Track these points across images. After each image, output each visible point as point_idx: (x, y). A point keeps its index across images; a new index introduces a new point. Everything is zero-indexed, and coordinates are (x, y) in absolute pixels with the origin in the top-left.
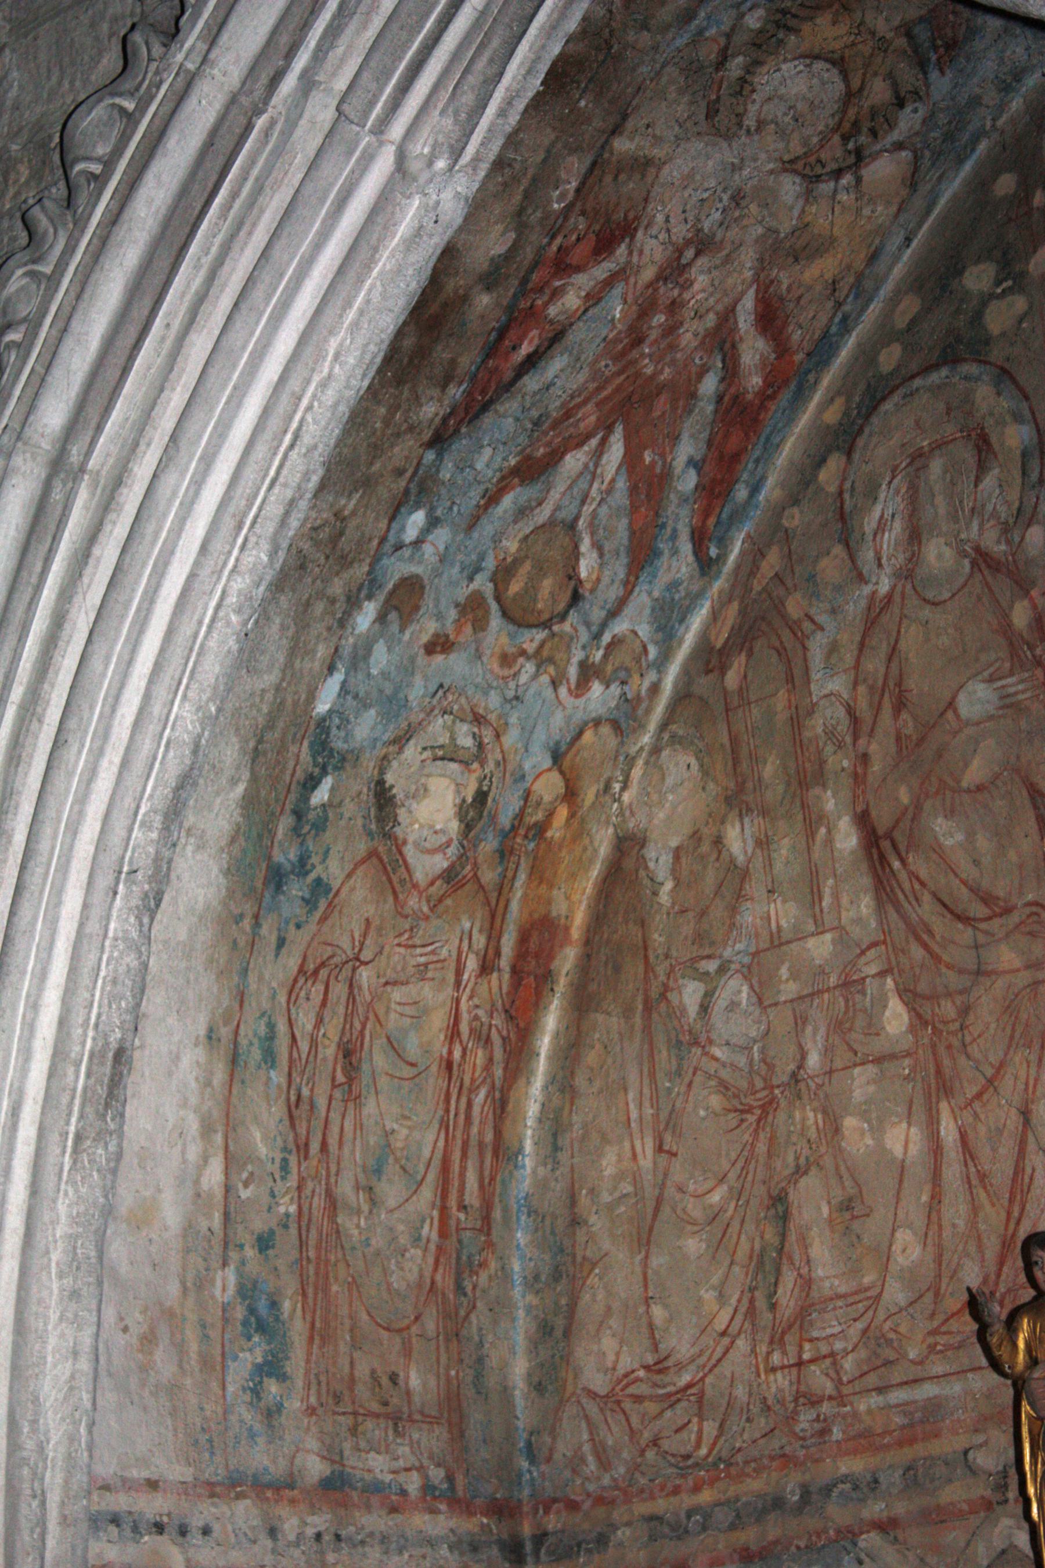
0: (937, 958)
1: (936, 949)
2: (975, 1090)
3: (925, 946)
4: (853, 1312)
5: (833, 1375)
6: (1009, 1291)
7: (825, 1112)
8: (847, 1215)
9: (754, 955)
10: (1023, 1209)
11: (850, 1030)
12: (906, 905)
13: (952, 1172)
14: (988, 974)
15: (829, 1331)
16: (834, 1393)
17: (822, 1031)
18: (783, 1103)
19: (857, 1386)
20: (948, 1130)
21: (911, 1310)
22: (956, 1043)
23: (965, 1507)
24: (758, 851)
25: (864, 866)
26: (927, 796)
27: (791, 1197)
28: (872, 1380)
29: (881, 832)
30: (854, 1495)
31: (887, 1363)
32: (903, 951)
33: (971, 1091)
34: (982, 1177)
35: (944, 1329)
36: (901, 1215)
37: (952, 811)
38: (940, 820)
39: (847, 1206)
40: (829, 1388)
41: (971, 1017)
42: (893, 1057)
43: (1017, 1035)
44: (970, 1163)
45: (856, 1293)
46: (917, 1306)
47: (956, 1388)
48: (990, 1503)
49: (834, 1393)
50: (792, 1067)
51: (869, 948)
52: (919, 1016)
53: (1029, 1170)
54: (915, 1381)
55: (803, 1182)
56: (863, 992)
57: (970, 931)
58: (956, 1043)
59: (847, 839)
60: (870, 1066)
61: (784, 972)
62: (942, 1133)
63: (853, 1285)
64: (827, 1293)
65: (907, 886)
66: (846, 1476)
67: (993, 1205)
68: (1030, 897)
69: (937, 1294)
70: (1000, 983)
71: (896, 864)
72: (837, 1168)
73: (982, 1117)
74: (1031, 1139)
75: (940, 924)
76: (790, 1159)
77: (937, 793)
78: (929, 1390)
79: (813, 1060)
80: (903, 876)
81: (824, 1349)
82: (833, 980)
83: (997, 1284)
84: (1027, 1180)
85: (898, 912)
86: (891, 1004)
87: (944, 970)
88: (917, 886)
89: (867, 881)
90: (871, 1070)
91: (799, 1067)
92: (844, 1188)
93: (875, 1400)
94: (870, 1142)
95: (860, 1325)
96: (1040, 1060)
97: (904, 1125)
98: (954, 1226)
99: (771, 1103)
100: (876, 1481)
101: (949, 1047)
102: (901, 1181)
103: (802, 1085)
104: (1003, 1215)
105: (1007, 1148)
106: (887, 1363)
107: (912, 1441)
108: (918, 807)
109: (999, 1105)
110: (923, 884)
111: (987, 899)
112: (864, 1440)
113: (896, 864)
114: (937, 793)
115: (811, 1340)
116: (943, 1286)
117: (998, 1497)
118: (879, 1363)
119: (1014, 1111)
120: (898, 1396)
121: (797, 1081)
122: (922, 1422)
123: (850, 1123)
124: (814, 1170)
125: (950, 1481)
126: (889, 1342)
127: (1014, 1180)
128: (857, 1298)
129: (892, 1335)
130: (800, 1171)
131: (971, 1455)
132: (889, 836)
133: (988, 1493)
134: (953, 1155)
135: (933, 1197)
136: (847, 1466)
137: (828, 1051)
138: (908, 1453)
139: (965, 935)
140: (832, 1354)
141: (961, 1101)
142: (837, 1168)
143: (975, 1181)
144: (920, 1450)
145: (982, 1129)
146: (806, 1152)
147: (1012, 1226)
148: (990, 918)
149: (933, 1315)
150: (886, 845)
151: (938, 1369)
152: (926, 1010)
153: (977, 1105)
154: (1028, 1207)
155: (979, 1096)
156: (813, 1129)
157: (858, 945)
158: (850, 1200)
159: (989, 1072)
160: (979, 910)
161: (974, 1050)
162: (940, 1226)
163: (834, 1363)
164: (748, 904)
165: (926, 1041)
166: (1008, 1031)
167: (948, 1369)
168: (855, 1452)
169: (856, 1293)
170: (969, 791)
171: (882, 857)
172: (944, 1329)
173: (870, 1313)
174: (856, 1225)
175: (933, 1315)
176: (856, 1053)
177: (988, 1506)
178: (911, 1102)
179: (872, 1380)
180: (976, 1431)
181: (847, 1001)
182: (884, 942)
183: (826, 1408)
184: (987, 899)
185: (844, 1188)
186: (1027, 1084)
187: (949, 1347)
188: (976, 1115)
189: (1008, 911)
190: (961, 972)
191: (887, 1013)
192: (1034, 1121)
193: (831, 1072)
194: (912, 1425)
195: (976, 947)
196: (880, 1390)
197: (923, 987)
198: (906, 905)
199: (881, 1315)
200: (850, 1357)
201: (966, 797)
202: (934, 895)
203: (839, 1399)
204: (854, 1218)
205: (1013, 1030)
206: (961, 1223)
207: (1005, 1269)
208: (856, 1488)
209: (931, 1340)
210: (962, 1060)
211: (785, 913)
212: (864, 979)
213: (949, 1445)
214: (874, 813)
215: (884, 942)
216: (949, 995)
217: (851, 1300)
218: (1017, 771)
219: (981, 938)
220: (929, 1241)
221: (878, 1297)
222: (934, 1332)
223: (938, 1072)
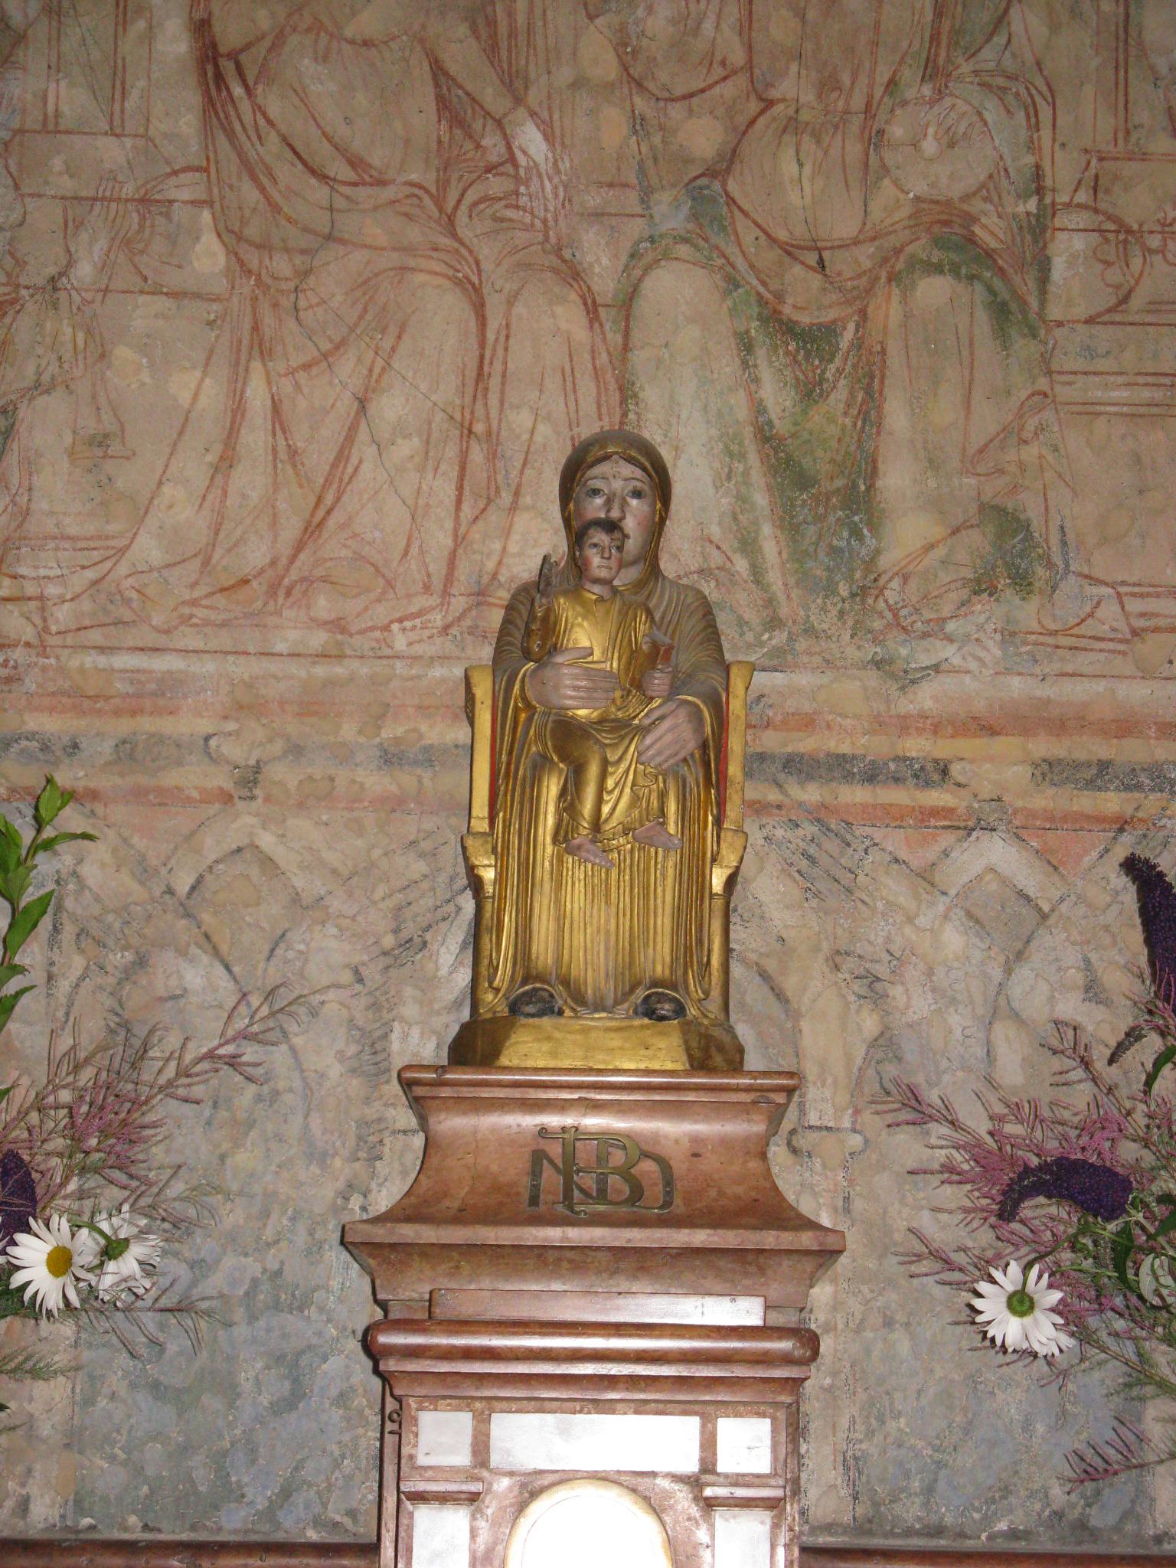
0: (276, 208)
1: (277, 197)
2: (302, 359)
3: (263, 190)
4: (83, 558)
5: (38, 621)
6: (303, 580)
7: (89, 332)
8: (99, 452)
9: (15, 132)
10: (338, 499)
11: (142, 252)
12: (243, 138)
13: (255, 438)
14: (341, 241)
15: (42, 572)
16: (35, 641)
17: (102, 244)
18: (30, 307)
19: (70, 640)
20: (257, 394)
21: (166, 573)
22: (286, 303)
23: (195, 794)
24: (45, 20)
25: (192, 79)
26: (294, 30)
27: (21, 413)
29: (222, 50)
30: (41, 756)
31: (119, 623)
32: (231, 187)
33: (297, 360)
34: (293, 453)
35: (203, 602)
36: (173, 469)
37: (326, 58)
38: (306, 61)
39: (101, 441)
40: (29, 634)
41: (311, 281)
42: (197, 296)
43: (369, 317)
44: (279, 433)
45: (91, 538)
46: (177, 571)
47: (209, 666)
48: (231, 797)
49: (35, 641)
50: (52, 270)
51: (184, 170)
52: (241, 263)
53: (354, 460)
55: (41, 401)
56: (168, 216)
57: (326, 190)
58: (286, 303)
59: (175, 43)
60: (164, 298)
61: (57, 163)
62: (248, 393)
63: (90, 528)
64: (50, 526)
65: (248, 117)
66: (34, 734)
67: (301, 486)
68: (414, 177)
69: (206, 563)
70: (358, 257)
71: (238, 91)
72: (94, 397)
73: (306, 391)
74: (363, 427)
75: (288, 173)
76: (30, 371)
77: (309, 30)
78: (161, 664)
79: (84, 271)
80: (245, 107)
81: (31, 589)
82: (128, 190)
83: (287, 569)
84: (350, 470)
85: (231, 143)
86: (204, 239)
87: (284, 222)
88: (261, 121)
89: (193, 97)
90: (162, 303)
91: (61, 274)
92: (99, 420)
94: (148, 380)
95: (90, 575)
96: (393, 349)
97: (198, 374)
98: (244, 496)
99: (13, 302)
100: (75, 746)
101: (275, 305)
102: (181, 433)
103: (62, 295)
104: (312, 500)
105: (331, 431)
106: (119, 623)
107: (134, 713)
108: (279, 39)
109: (331, 383)
110: (270, 123)
111: (355, 162)
112: (80, 699)
113: (238, 91)
114: (309, 30)
115: (14, 577)
116: (216, 557)
117: (246, 793)
119: (348, 394)
120: (123, 661)
121: (55, 289)
122: (154, 694)
123: (123, 353)
124: (60, 392)
126: (127, 602)
127: (334, 465)
128: (92, 544)
130: (39, 388)
131: (213, 743)
132: (234, 56)
133: (229, 786)
134: (259, 421)
136: (36, 722)
137: (104, 266)
138: (124, 726)
139: (321, 193)
140: (41, 598)
141: (281, 367)
142: (94, 397)
143: (283, 455)
144: (147, 724)
145: (302, 404)
146: (53, 368)
147: (321, 513)
148: (355, 184)
149: (194, 585)
150: (228, 67)
151: (193, 642)
152: (253, 258)
153: (302, 376)
154: (345, 498)
155: (306, 367)
156: (70, 346)
157: (168, 163)
158: (106, 436)
159: (326, 346)
160: (340, 170)
161: (307, 316)
162: (225, 493)
163: (43, 609)
164: (19, 74)
165: (246, 290)
166: (360, 307)
167: (200, 644)
168: (52, 710)
169: (91, 538)
170: (352, 42)
171: (219, 78)
172: (203, 602)
173: (108, 564)
174: (109, 466)
175: (194, 585)
176: (145, 279)
177: (227, 798)
178: (211, 351)
179: (95, 636)
180: (226, 718)
181: (143, 218)
182: (206, 170)
183: (18, 654)
184: (355, 162)
185: (99, 420)
186: (371, 370)
187: (207, 623)
188: (297, 386)
189: (381, 183)
190: (306, 230)
191: (198, 248)
192: (372, 409)
193: (106, 291)
194: (139, 696)
195: (331, 209)
196: (102, 650)
197: (252, 231)
198: (243, 138)
199: (123, 569)
200: (66, 606)
201: (345, 46)
202: (285, 140)
203: (43, 650)
204: (105, 456)
205: (365, 310)
206: (254, 496)
207: (302, 556)
208: (45, 748)
209: (186, 610)
210: (291, 324)
211: (71, 99)
212: (171, 202)
213: (187, 725)
214: (217, 27)
215: (206, 170)
216: (286, 250)
217: (80, 545)
218: (422, 41)
219: (340, 203)
220: (206, 504)
221: (123, 551)
222: (194, 603)
223: (256, 328)
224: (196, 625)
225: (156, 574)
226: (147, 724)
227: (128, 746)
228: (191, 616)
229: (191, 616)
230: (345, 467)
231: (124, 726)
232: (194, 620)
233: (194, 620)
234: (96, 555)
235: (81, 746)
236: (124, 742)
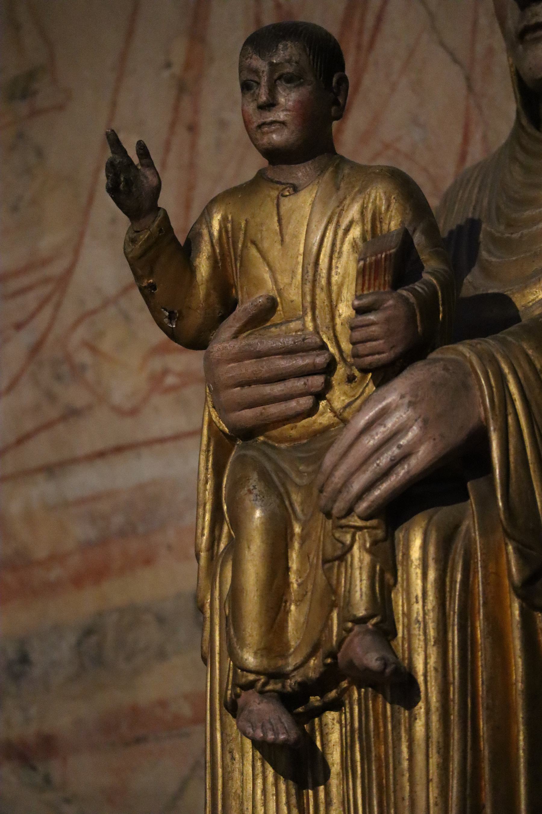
8: (23, 108)
28: (40, 450)
31: (72, 414)
54: (119, 450)
93: (41, 490)
100: (24, 659)
106: (72, 414)
118: (53, 413)
125: (162, 655)
126: (77, 371)
128: (25, 281)
129: (84, 357)
135: (188, 66)
138: (85, 604)
144: (116, 592)
194: (103, 542)
196: (51, 470)
199: (69, 312)
204: (34, 113)
221: (63, 281)
224: (173, 389)
225: (112, 311)
226: (116, 592)
227: (93, 639)
228: (165, 372)
229: (165, 372)
230: (362, 20)
231: (85, 604)
232: (170, 380)
233: (170, 380)
234: (31, 300)
235: (34, 656)
236: (88, 632)
